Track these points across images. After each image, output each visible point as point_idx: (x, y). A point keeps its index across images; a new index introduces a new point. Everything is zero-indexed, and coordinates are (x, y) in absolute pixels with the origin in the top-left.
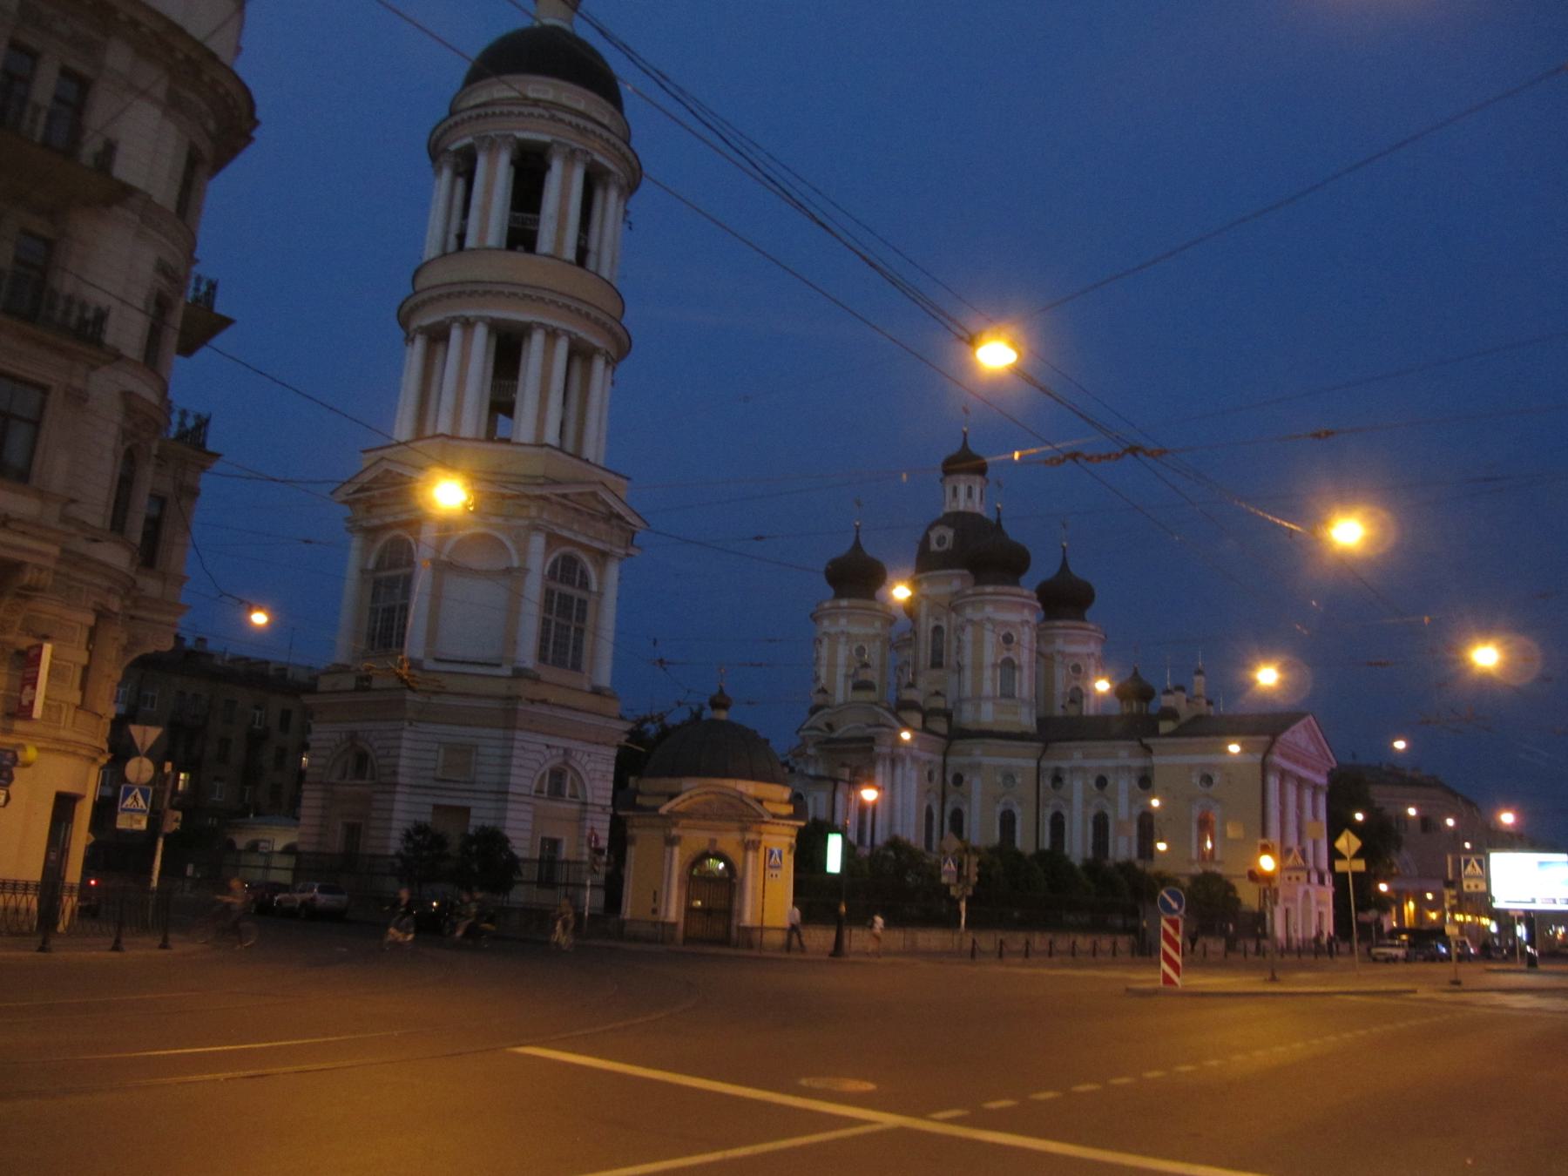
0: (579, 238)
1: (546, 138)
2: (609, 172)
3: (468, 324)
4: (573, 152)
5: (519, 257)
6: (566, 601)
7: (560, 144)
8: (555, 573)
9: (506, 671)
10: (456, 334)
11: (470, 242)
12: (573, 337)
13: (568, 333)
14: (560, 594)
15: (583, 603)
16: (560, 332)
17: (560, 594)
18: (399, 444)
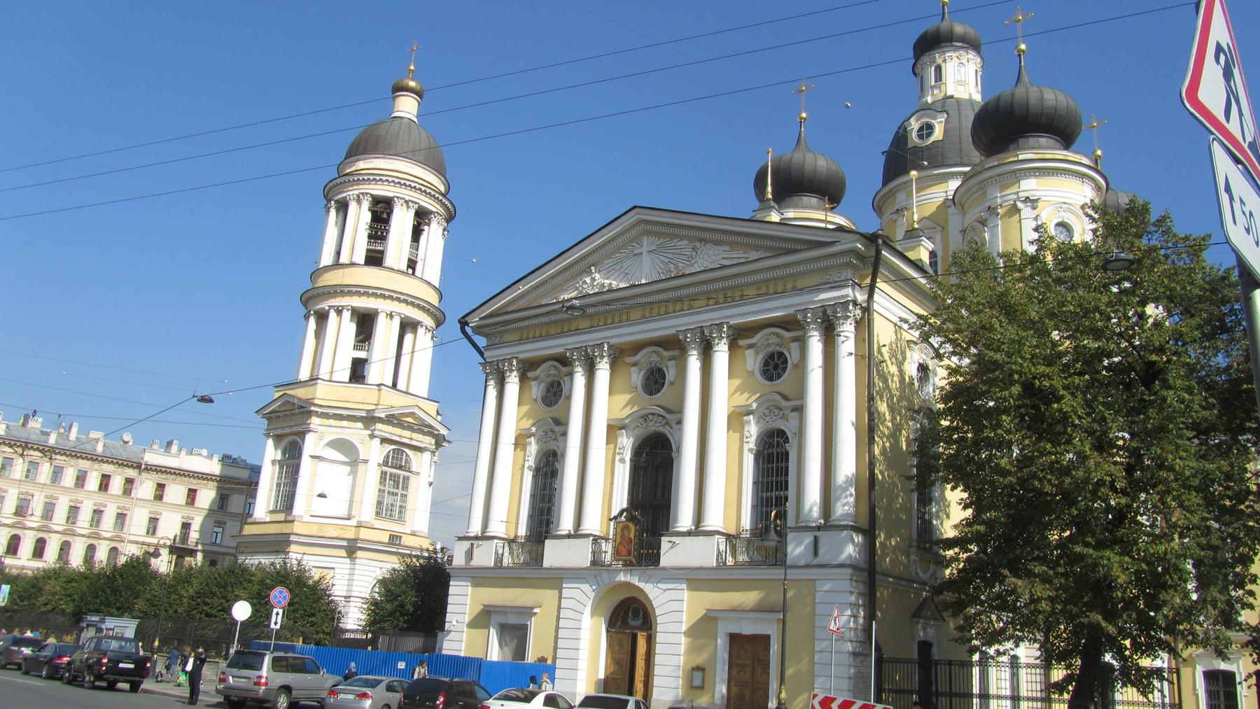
0: (411, 253)
1: (391, 195)
2: (431, 212)
3: (339, 312)
4: (407, 202)
5: (373, 271)
6: (395, 479)
7: (398, 198)
8: (387, 462)
9: (353, 522)
10: (333, 315)
11: (344, 259)
12: (403, 316)
13: (399, 314)
14: (391, 474)
15: (406, 479)
16: (394, 314)
17: (391, 474)
18: (300, 382)
